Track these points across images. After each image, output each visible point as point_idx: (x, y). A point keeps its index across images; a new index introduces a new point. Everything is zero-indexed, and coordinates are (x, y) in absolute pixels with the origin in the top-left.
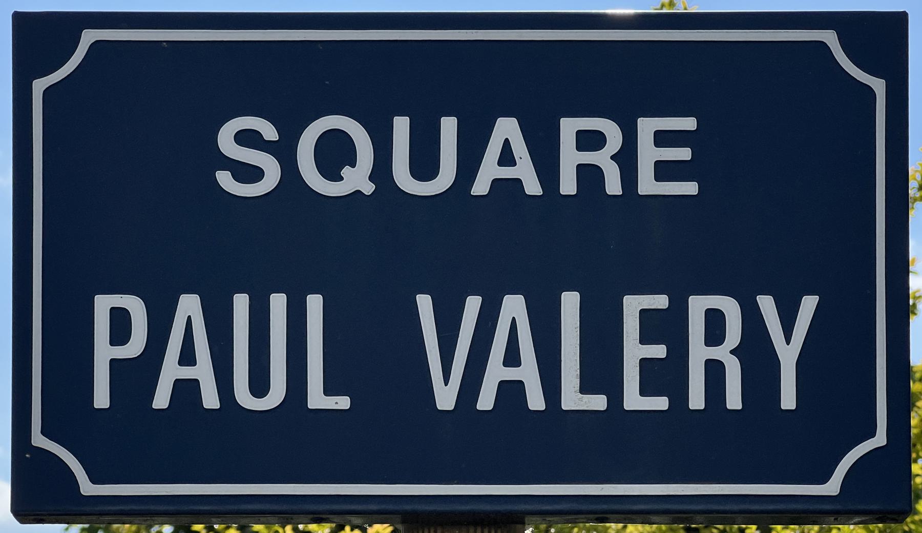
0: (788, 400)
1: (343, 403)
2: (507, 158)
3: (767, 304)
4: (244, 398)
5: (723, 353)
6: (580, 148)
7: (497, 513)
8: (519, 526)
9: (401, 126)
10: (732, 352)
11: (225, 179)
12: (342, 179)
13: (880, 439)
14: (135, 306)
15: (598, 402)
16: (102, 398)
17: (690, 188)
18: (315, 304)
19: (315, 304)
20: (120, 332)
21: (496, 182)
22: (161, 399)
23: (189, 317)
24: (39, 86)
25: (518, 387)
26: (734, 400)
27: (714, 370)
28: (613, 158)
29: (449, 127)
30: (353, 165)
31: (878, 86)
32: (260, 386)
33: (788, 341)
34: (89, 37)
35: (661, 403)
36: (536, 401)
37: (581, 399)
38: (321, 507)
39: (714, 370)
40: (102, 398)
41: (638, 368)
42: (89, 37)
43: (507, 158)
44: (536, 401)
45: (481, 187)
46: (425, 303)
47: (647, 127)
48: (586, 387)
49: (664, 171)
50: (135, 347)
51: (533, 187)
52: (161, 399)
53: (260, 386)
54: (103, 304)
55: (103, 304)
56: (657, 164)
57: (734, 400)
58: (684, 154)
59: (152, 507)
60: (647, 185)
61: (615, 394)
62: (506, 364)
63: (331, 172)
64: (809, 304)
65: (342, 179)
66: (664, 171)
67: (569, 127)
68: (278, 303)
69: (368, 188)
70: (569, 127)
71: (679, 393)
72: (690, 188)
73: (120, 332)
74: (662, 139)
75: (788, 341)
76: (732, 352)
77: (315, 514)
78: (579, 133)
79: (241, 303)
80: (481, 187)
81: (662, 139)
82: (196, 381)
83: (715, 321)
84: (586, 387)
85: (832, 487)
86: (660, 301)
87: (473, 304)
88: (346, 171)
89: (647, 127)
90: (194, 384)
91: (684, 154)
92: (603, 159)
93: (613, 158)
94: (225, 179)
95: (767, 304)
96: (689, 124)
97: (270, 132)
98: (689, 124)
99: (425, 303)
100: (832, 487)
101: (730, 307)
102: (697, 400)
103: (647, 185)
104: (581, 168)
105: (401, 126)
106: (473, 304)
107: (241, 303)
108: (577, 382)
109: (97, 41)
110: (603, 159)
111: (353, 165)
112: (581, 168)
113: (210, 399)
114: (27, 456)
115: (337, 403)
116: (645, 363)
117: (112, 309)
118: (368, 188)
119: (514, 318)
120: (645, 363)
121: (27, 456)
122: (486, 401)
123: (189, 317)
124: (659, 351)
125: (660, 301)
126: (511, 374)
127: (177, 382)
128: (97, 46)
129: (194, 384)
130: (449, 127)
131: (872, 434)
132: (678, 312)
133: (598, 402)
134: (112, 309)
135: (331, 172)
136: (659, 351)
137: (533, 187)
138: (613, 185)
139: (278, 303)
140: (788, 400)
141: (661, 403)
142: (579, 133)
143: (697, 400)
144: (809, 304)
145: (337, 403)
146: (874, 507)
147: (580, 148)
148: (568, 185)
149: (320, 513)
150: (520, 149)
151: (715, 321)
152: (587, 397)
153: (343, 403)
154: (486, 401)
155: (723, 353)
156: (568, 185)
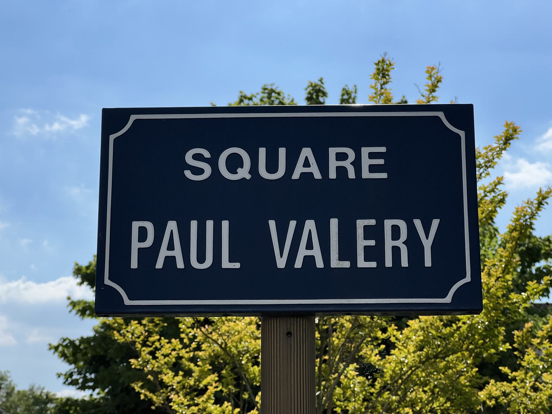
0: (428, 263)
1: (237, 265)
2: (307, 164)
3: (418, 223)
4: (195, 263)
5: (399, 243)
6: (337, 160)
7: (302, 312)
8: (313, 317)
9: (262, 152)
10: (403, 243)
11: (188, 174)
12: (237, 173)
13: (468, 279)
14: (149, 226)
15: (346, 264)
16: (134, 264)
17: (384, 175)
18: (225, 225)
19: (225, 225)
20: (143, 235)
21: (302, 174)
22: (159, 265)
23: (172, 230)
24: (112, 137)
25: (312, 258)
26: (405, 263)
27: (396, 251)
28: (351, 163)
29: (282, 152)
30: (242, 168)
31: (462, 134)
32: (201, 259)
33: (427, 238)
34: (133, 118)
35: (373, 265)
36: (320, 264)
37: (339, 263)
38: (227, 310)
39: (396, 251)
40: (134, 264)
41: (363, 250)
42: (133, 118)
43: (307, 164)
44: (320, 264)
45: (296, 176)
46: (272, 224)
47: (365, 151)
48: (341, 258)
49: (373, 169)
50: (149, 243)
51: (318, 175)
52: (159, 265)
53: (201, 259)
54: (136, 225)
55: (136, 225)
56: (370, 166)
57: (405, 263)
58: (381, 162)
59: (155, 310)
60: (366, 174)
61: (354, 260)
62: (307, 248)
63: (232, 169)
64: (436, 223)
65: (237, 173)
66: (373, 169)
67: (333, 152)
68: (210, 224)
69: (248, 177)
70: (333, 152)
71: (381, 260)
72: (384, 175)
73: (143, 235)
74: (372, 156)
75: (427, 238)
76: (403, 243)
77: (225, 312)
78: (337, 154)
79: (194, 225)
80: (296, 176)
81: (372, 156)
82: (174, 257)
83: (396, 231)
84: (341, 258)
85: (448, 299)
86: (373, 222)
87: (293, 224)
88: (239, 170)
89: (365, 151)
90: (174, 258)
91: (381, 162)
92: (347, 164)
93: (351, 163)
94: (188, 174)
95: (418, 223)
96: (383, 149)
97: (207, 154)
98: (383, 149)
99: (272, 224)
100: (448, 299)
101: (402, 225)
102: (389, 263)
103: (366, 174)
104: (338, 168)
105: (262, 152)
106: (293, 224)
107: (194, 225)
108: (337, 256)
109: (136, 119)
110: (347, 164)
111: (242, 168)
112: (338, 168)
113: (180, 265)
114: (102, 288)
115: (234, 266)
116: (366, 248)
117: (139, 227)
118: (248, 177)
119: (310, 230)
120: (366, 248)
121: (102, 288)
122: (298, 264)
123: (172, 230)
124: (372, 243)
125: (373, 222)
126: (309, 253)
127: (166, 257)
128: (136, 121)
129: (174, 258)
130: (282, 152)
131: (464, 277)
132: (380, 227)
133: (346, 264)
134: (139, 227)
135: (232, 169)
136: (372, 243)
137: (318, 175)
138: (352, 174)
139: (210, 224)
140: (428, 263)
141: (373, 265)
142: (337, 154)
143: (389, 263)
144: (436, 223)
145: (234, 266)
146: (468, 308)
147: (337, 160)
148: (333, 175)
149: (227, 312)
150: (312, 160)
151: (396, 231)
152: (341, 262)
153: (237, 265)
154: (298, 264)
155: (399, 243)
156: (333, 175)
